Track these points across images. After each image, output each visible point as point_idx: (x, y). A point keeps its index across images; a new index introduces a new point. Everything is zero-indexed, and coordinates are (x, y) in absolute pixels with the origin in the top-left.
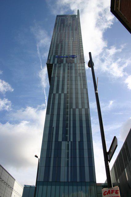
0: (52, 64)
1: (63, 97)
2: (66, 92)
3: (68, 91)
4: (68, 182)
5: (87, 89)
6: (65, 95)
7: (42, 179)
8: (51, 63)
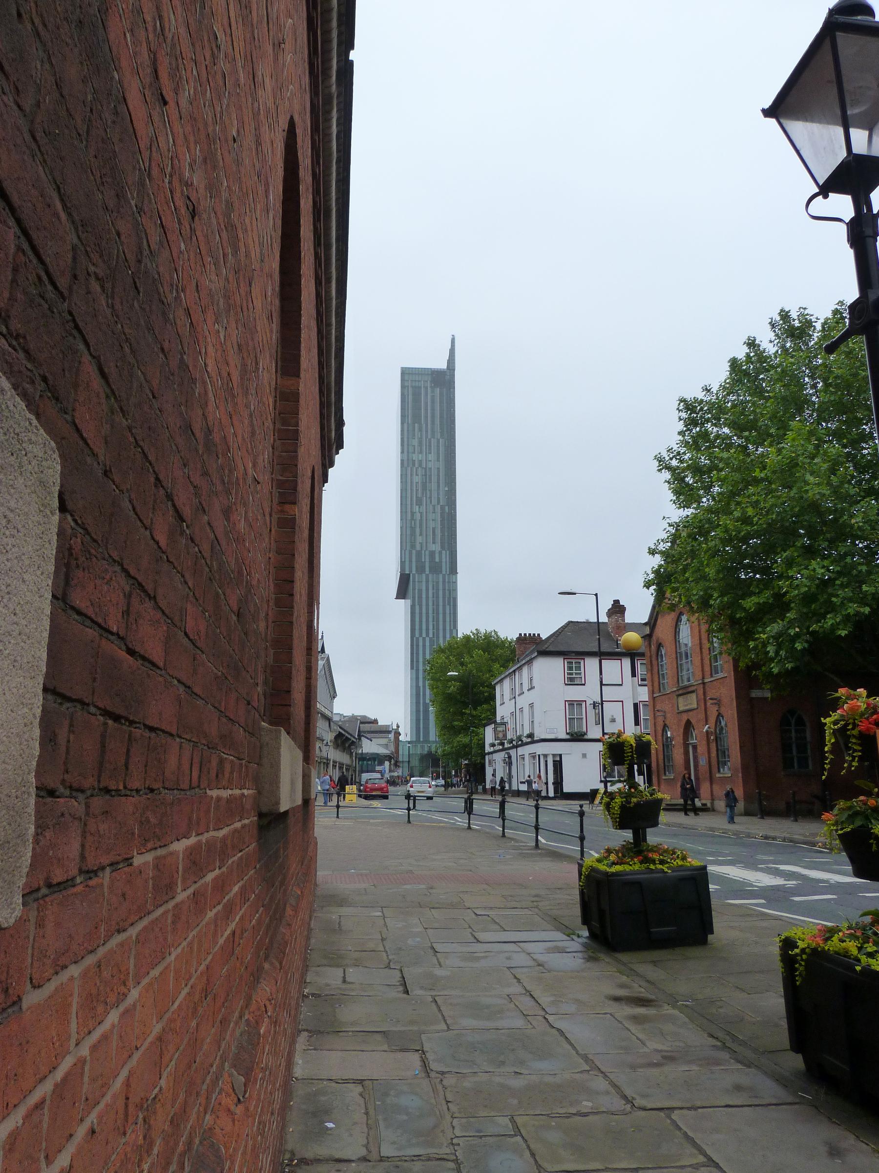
1: (428, 644)
2: (431, 635)
6: (431, 639)
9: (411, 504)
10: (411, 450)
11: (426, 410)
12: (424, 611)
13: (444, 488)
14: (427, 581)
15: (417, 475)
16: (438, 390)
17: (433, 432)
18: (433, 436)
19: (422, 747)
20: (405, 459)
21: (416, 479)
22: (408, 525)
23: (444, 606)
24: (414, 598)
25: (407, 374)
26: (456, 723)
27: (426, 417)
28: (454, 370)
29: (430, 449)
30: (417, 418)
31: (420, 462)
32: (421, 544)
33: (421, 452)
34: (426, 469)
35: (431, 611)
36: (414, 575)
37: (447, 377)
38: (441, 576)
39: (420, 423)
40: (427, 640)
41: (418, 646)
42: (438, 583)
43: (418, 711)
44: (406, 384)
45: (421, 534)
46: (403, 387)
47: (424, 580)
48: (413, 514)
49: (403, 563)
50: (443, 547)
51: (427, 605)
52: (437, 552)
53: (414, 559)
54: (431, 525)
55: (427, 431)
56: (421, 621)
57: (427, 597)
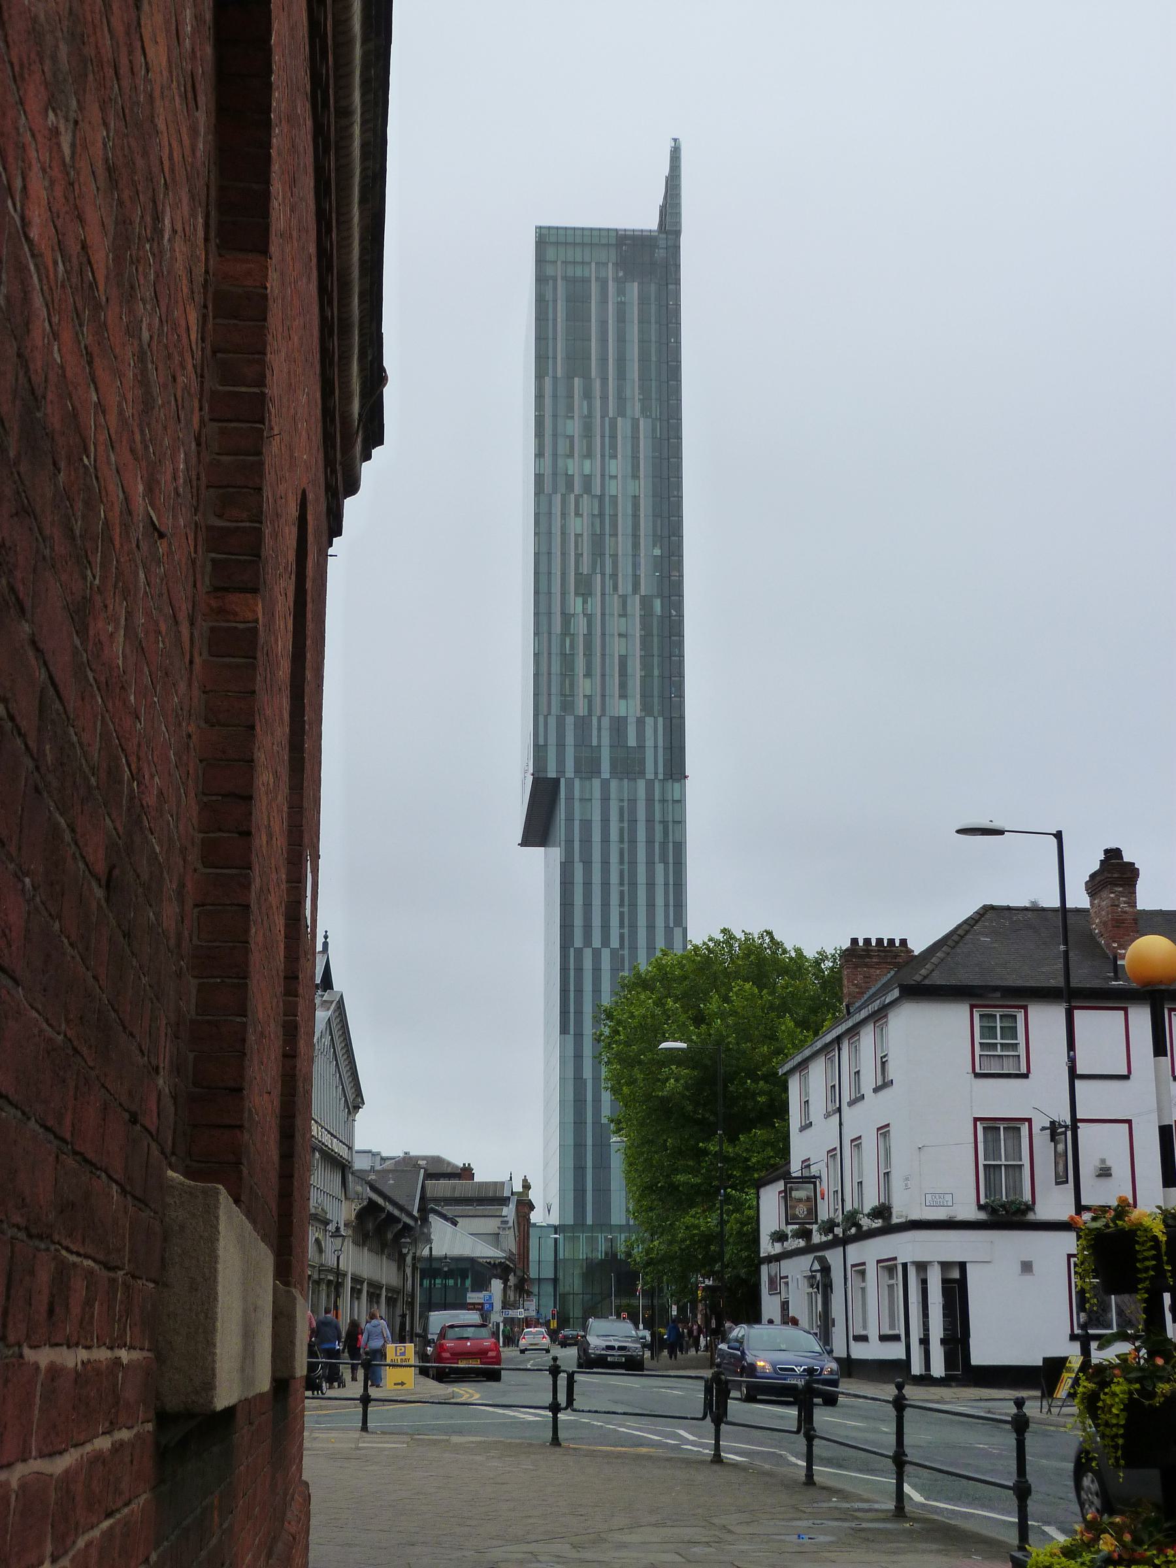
0: (556, 781)
1: (606, 964)
2: (615, 943)
3: (622, 936)
4: (628, 1225)
5: (685, 930)
6: (614, 952)
7: (570, 1221)
8: (552, 774)
9: (564, 594)
10: (562, 448)
11: (603, 340)
12: (597, 878)
13: (649, 551)
14: (605, 799)
15: (578, 514)
16: (634, 289)
17: (621, 399)
18: (621, 412)
19: (592, 1241)
20: (548, 472)
21: (576, 525)
22: (555, 649)
23: (650, 864)
24: (569, 842)
25: (550, 242)
26: (681, 1178)
27: (603, 360)
28: (678, 233)
29: (614, 446)
30: (577, 362)
31: (587, 480)
32: (589, 698)
33: (589, 455)
34: (601, 498)
35: (614, 879)
36: (570, 783)
37: (660, 254)
38: (641, 784)
39: (586, 377)
40: (606, 954)
41: (579, 970)
42: (633, 801)
43: (579, 1146)
44: (550, 271)
45: (588, 674)
46: (541, 279)
47: (597, 794)
48: (567, 617)
49: (539, 751)
50: (647, 708)
51: (605, 863)
52: (632, 721)
53: (570, 740)
54: (617, 647)
55: (604, 398)
56: (588, 905)
57: (605, 840)
